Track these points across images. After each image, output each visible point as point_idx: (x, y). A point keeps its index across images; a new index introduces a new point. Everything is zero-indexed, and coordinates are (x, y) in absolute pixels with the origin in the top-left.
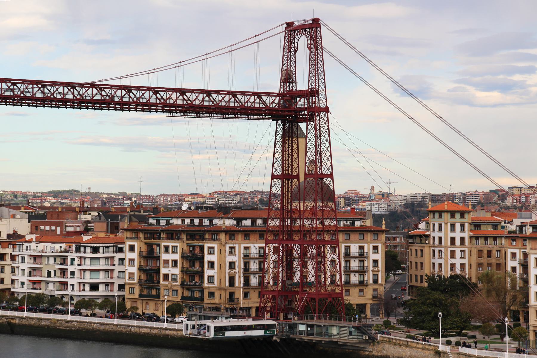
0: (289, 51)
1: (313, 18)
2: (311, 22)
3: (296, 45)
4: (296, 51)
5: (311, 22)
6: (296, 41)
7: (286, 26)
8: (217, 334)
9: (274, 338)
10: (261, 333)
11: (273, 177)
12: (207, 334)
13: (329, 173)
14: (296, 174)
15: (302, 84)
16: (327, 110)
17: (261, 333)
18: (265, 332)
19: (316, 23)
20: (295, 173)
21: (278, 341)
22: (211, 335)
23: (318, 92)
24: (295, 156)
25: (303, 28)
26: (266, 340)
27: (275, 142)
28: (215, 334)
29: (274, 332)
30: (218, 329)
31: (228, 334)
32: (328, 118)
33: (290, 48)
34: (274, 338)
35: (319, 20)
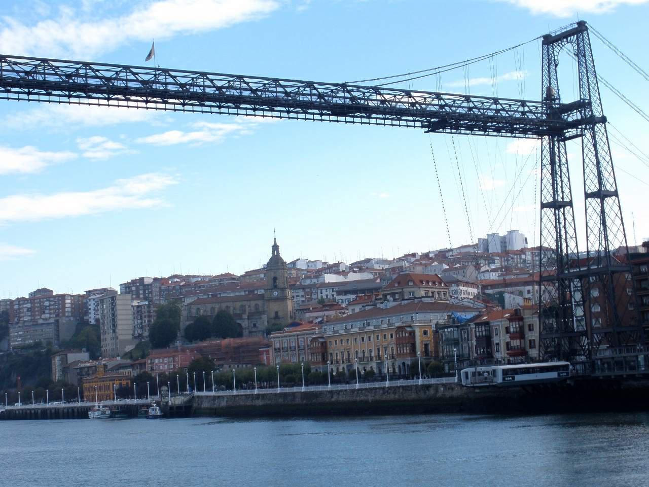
0: (549, 64)
1: (577, 21)
2: (576, 26)
3: (556, 58)
4: (556, 65)
5: (576, 26)
6: (556, 54)
7: (542, 39)
8: (506, 379)
9: (568, 382)
10: (554, 375)
11: (543, 206)
12: (495, 379)
13: (613, 190)
14: (568, 200)
15: (568, 95)
16: (603, 120)
17: (554, 375)
18: (559, 374)
19: (581, 28)
20: (567, 199)
21: (572, 384)
22: (499, 379)
23: (590, 104)
24: (565, 180)
25: (564, 36)
26: (560, 381)
27: (542, 166)
28: (504, 379)
29: (568, 374)
30: (505, 372)
31: (519, 378)
32: (605, 128)
33: (550, 63)
34: (568, 382)
35: (585, 23)
